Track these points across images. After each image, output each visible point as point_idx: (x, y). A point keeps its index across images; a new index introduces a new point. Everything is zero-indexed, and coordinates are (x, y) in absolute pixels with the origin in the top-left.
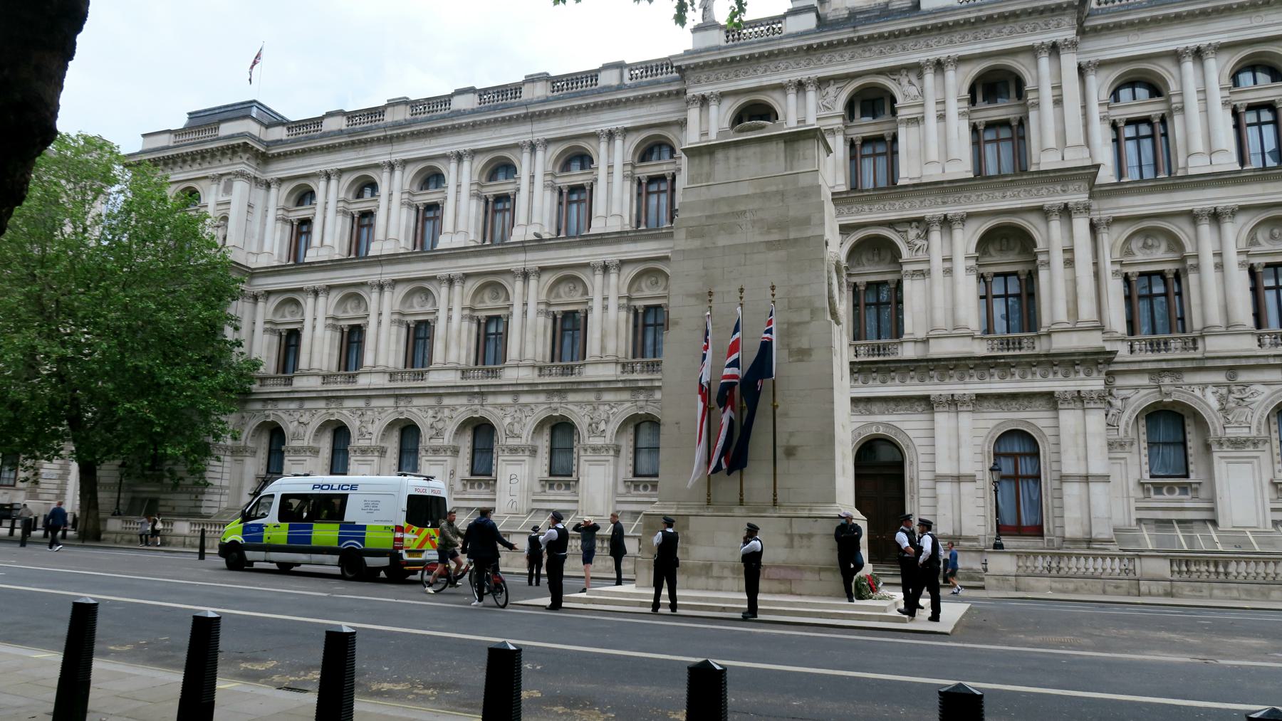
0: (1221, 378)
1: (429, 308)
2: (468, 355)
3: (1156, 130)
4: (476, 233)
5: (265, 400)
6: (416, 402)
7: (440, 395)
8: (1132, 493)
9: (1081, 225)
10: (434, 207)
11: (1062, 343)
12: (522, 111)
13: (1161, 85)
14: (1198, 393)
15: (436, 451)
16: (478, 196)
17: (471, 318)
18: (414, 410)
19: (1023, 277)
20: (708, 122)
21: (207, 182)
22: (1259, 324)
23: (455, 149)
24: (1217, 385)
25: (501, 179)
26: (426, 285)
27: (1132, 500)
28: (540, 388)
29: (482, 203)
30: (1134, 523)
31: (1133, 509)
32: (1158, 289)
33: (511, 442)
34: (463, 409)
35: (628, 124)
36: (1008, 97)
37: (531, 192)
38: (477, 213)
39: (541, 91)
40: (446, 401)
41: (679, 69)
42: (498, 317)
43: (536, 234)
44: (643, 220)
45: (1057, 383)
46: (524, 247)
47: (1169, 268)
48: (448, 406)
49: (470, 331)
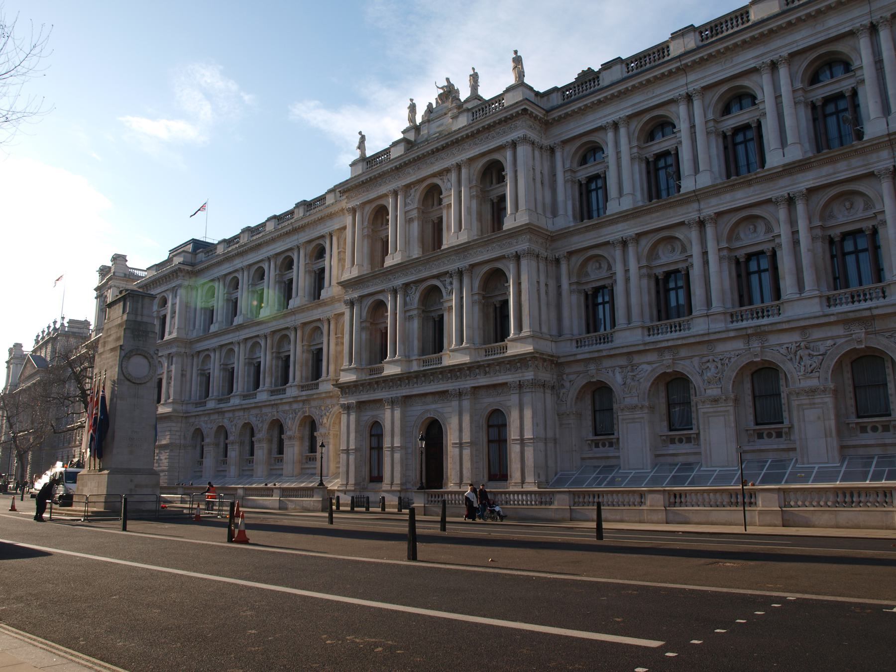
0: (622, 361)
5: (195, 416)
14: (611, 373)
21: (168, 292)
24: (621, 367)
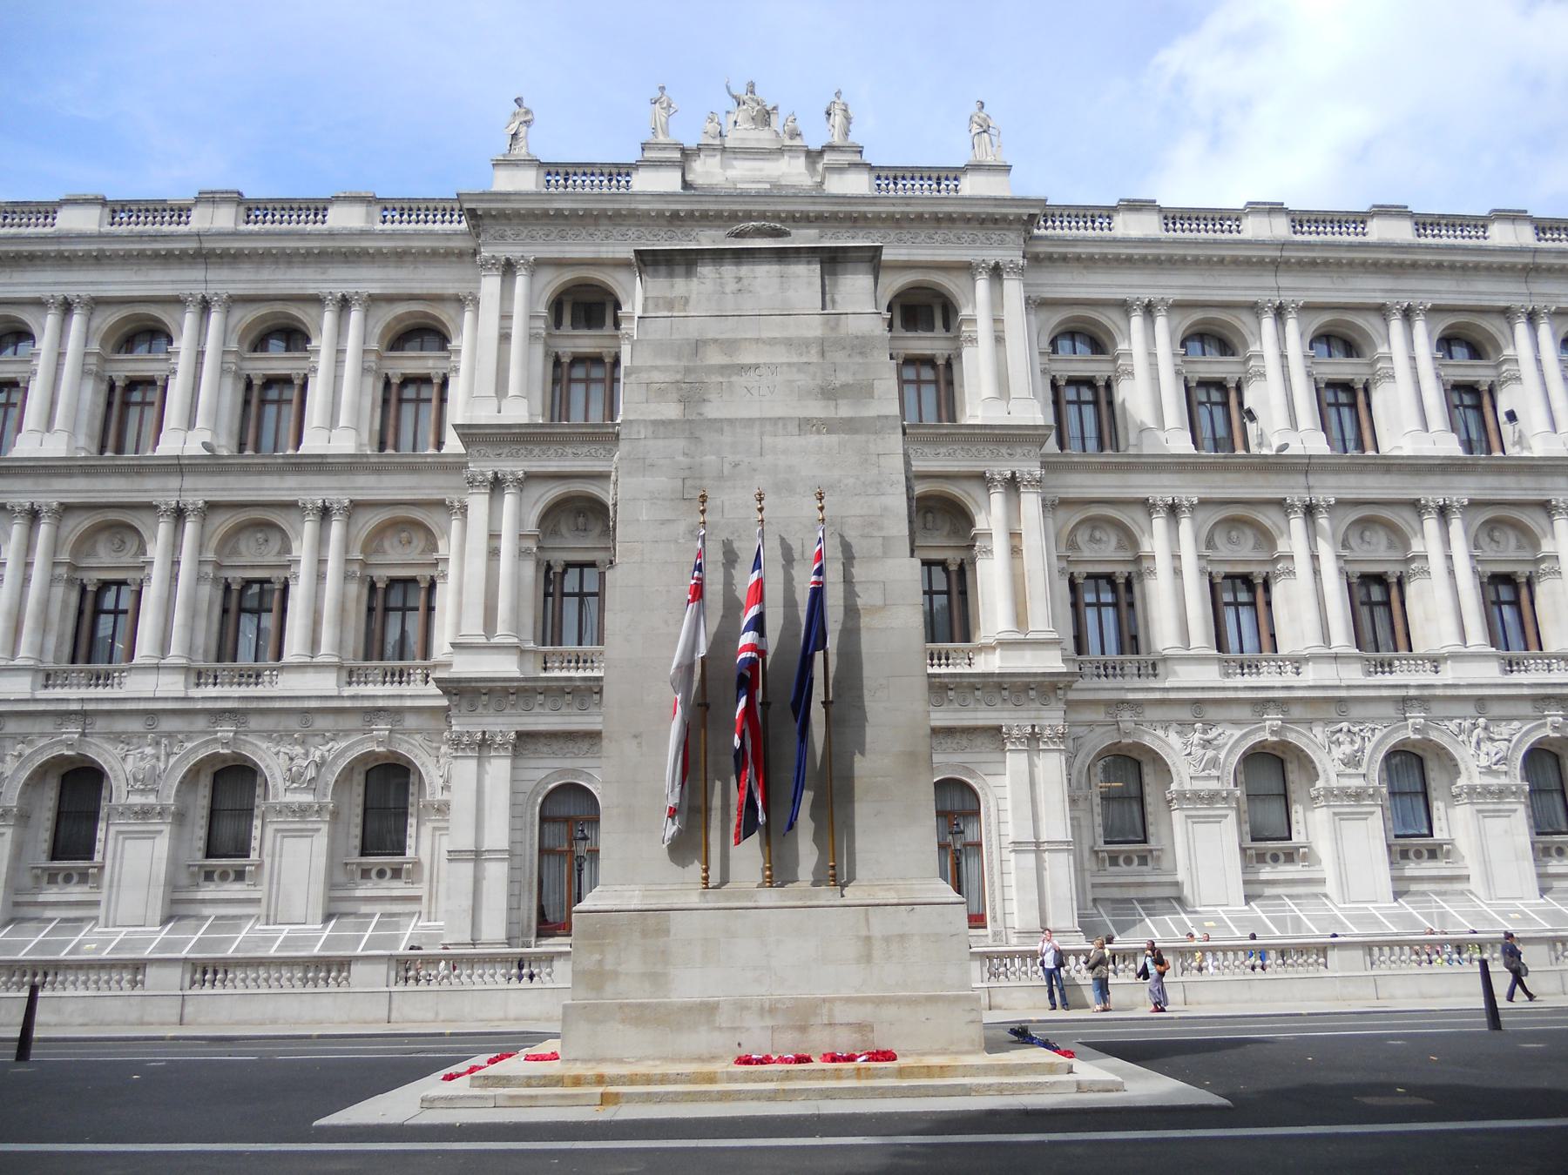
3: (1100, 394)
4: (90, 436)
8: (1087, 865)
9: (1031, 503)
11: (991, 663)
12: (192, 245)
13: (1104, 338)
17: (70, 581)
19: (953, 568)
20: (512, 299)
22: (1221, 645)
23: (60, 292)
25: (141, 352)
27: (1087, 875)
28: (199, 705)
29: (104, 387)
30: (1090, 904)
31: (1088, 886)
32: (1107, 597)
33: (136, 799)
35: (376, 289)
36: (931, 328)
39: (224, 218)
41: (472, 214)
42: (120, 583)
43: (205, 445)
44: (390, 440)
45: (1005, 714)
46: (179, 467)
47: (1121, 570)
49: (65, 604)
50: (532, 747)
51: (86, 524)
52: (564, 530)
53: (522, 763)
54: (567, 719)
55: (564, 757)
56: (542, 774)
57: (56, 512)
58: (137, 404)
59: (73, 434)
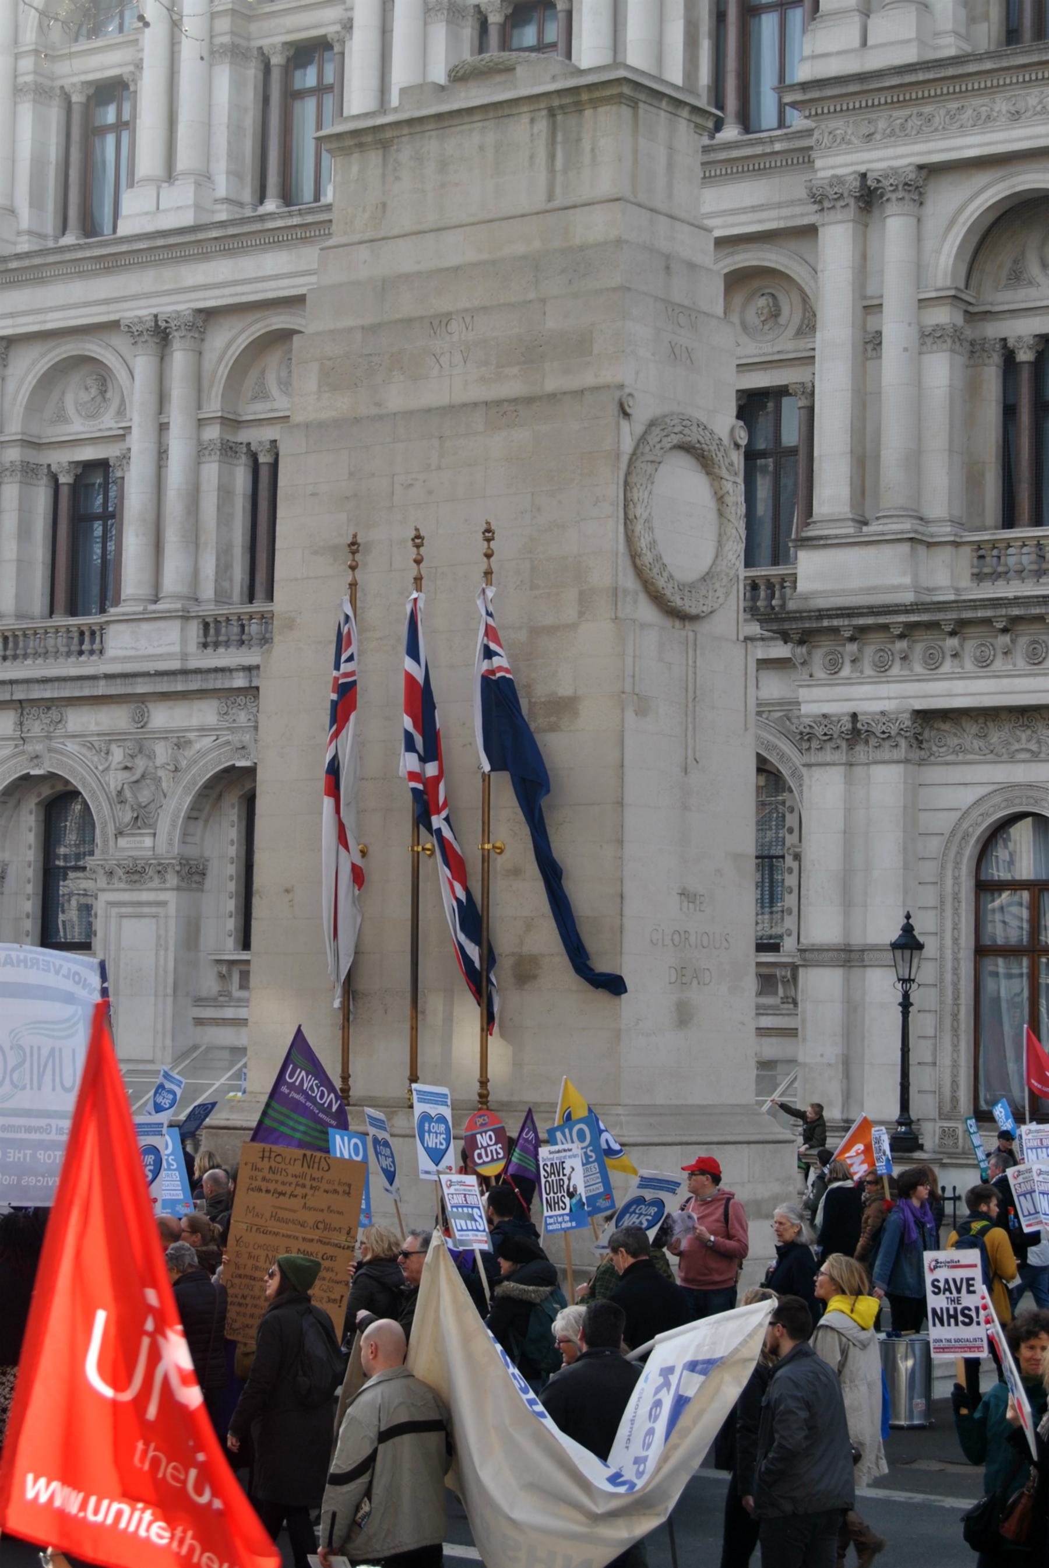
1: (108, 423)
2: (223, 569)
4: (235, 174)
6: (79, 720)
7: (142, 698)
10: (113, 90)
15: (136, 873)
16: (236, 53)
18: (71, 747)
26: (92, 348)
34: (207, 742)
37: (385, 32)
38: (236, 107)
40: (161, 717)
48: (164, 735)
49: (225, 492)
50: (953, 741)
51: (243, 342)
52: (1034, 268)
53: (933, 774)
54: (1005, 683)
55: (1012, 760)
56: (966, 797)
57: (191, 327)
58: (310, 92)
59: (204, 178)
